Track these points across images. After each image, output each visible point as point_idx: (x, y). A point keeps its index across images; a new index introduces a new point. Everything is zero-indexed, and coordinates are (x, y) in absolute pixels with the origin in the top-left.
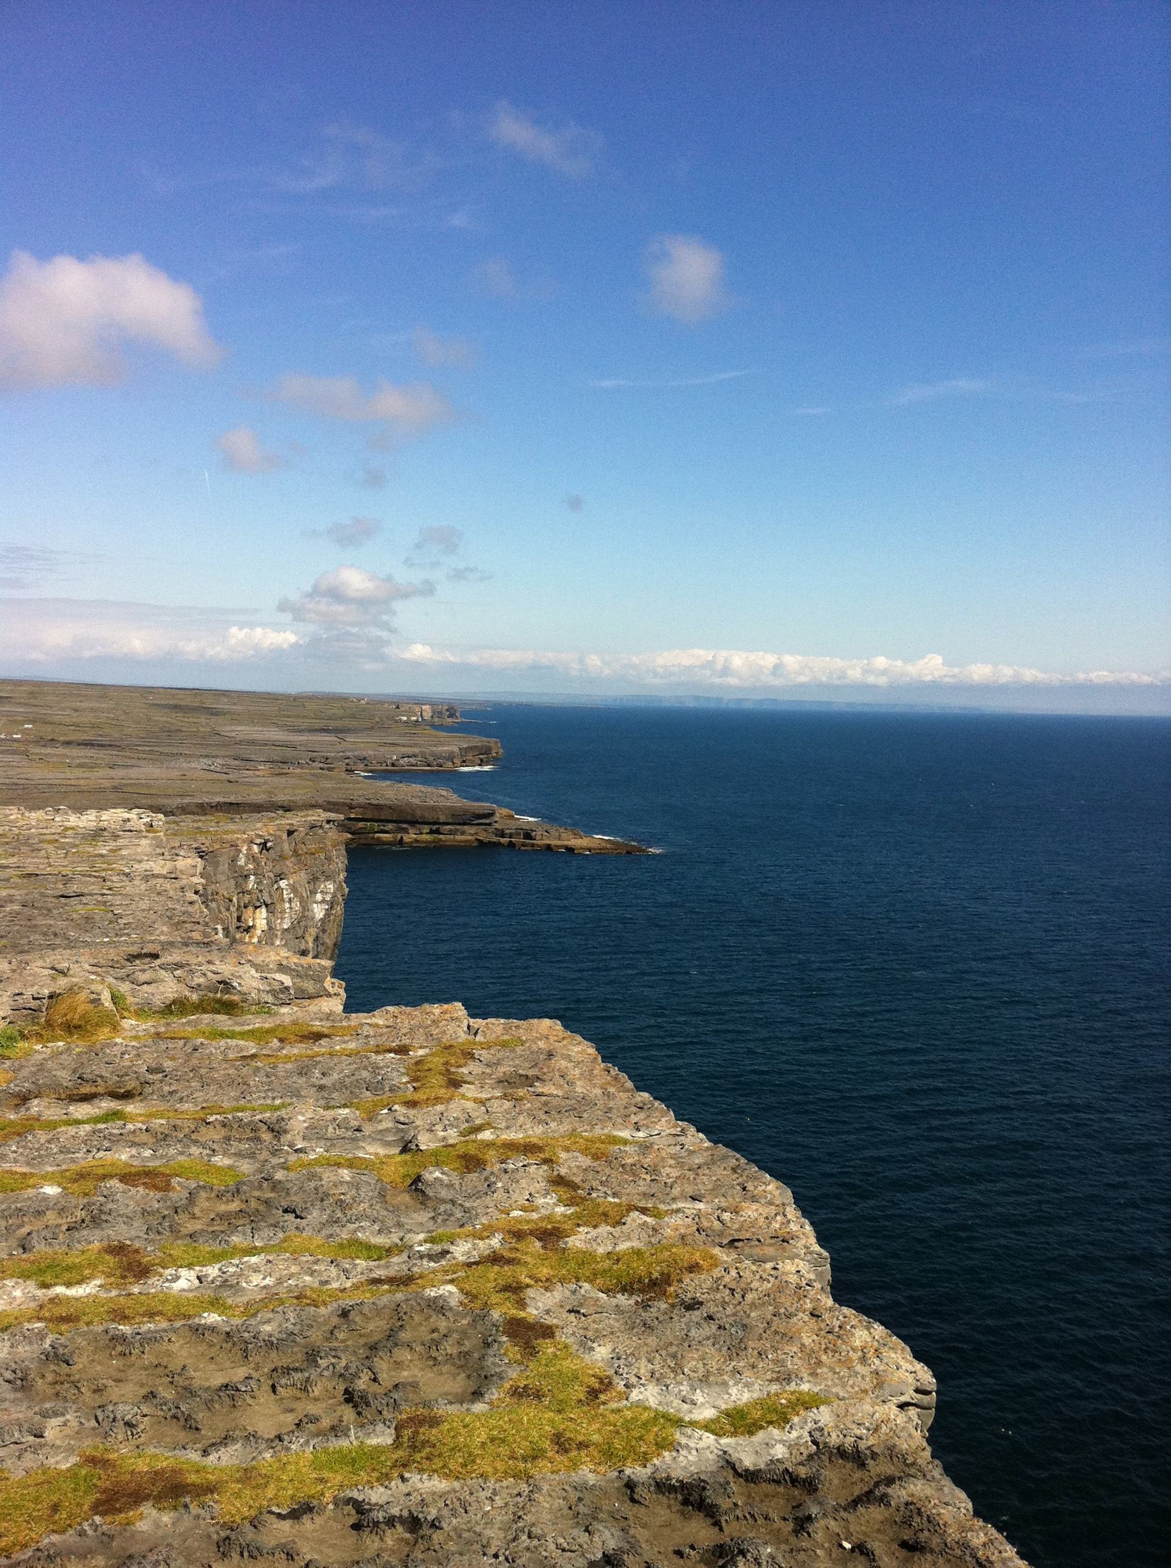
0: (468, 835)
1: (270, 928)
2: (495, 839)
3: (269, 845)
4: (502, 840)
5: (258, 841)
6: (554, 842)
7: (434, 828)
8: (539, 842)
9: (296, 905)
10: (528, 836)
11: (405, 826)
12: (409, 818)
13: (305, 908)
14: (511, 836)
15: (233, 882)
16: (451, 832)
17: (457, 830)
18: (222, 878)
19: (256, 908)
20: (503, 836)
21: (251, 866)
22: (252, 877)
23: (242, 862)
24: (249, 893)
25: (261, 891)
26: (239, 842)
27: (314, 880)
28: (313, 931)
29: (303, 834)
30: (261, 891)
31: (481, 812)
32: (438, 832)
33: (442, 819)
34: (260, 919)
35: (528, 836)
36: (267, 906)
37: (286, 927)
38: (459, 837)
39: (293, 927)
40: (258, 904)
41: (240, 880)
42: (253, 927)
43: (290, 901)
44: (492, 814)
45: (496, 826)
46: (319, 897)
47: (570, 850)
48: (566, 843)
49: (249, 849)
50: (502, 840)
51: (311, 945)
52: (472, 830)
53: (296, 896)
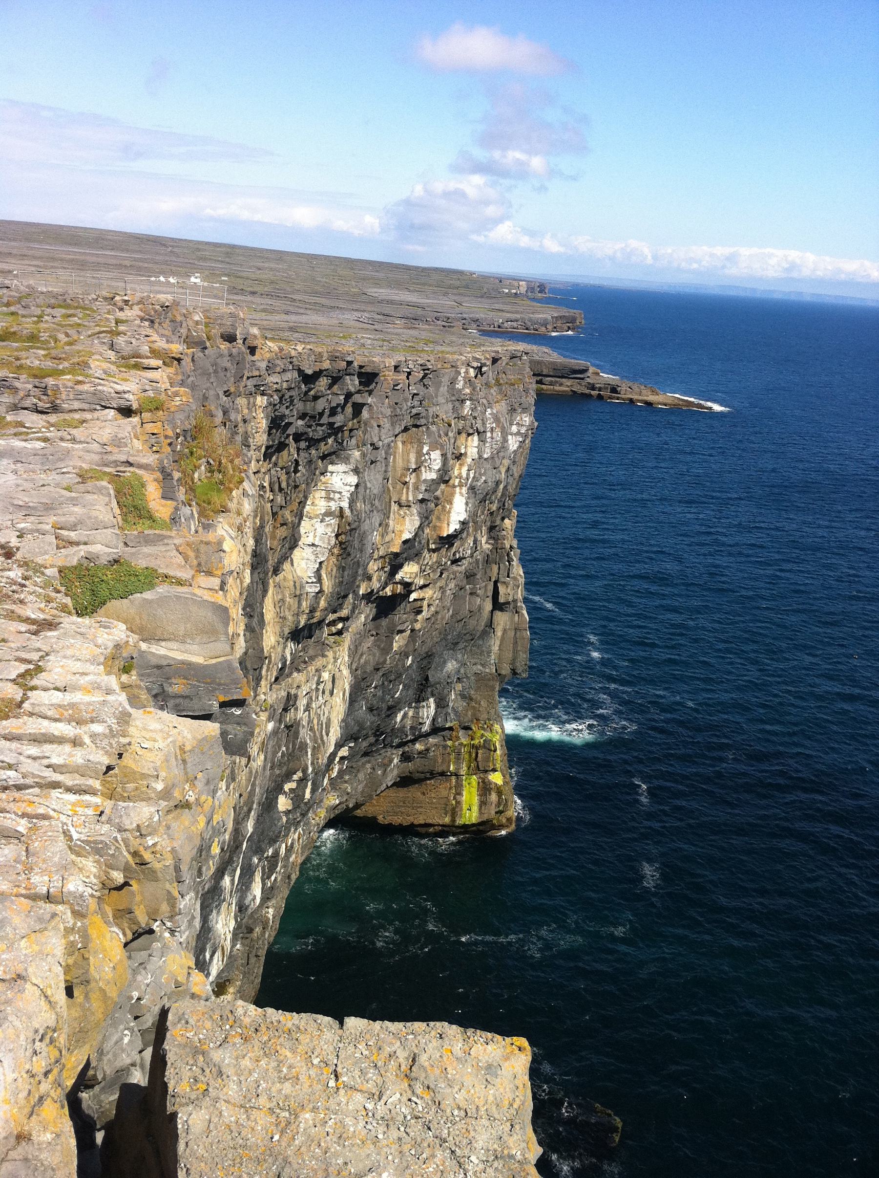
0: (566, 386)
2: (587, 391)
4: (593, 393)
5: (475, 364)
6: (635, 397)
8: (623, 396)
9: (498, 435)
10: (614, 390)
13: (505, 440)
14: (600, 389)
15: (450, 406)
17: (557, 382)
18: (441, 400)
19: (469, 435)
20: (593, 388)
21: (468, 391)
22: (468, 403)
23: (460, 385)
24: (464, 418)
25: (475, 418)
27: (512, 410)
28: (506, 462)
31: (577, 368)
33: (545, 372)
34: (471, 447)
35: (614, 390)
36: (479, 433)
38: (557, 388)
40: (471, 431)
41: (457, 404)
42: (466, 453)
44: (585, 371)
45: (588, 380)
46: (514, 429)
47: (649, 404)
48: (645, 398)
49: (467, 372)
50: (593, 393)
52: (568, 382)
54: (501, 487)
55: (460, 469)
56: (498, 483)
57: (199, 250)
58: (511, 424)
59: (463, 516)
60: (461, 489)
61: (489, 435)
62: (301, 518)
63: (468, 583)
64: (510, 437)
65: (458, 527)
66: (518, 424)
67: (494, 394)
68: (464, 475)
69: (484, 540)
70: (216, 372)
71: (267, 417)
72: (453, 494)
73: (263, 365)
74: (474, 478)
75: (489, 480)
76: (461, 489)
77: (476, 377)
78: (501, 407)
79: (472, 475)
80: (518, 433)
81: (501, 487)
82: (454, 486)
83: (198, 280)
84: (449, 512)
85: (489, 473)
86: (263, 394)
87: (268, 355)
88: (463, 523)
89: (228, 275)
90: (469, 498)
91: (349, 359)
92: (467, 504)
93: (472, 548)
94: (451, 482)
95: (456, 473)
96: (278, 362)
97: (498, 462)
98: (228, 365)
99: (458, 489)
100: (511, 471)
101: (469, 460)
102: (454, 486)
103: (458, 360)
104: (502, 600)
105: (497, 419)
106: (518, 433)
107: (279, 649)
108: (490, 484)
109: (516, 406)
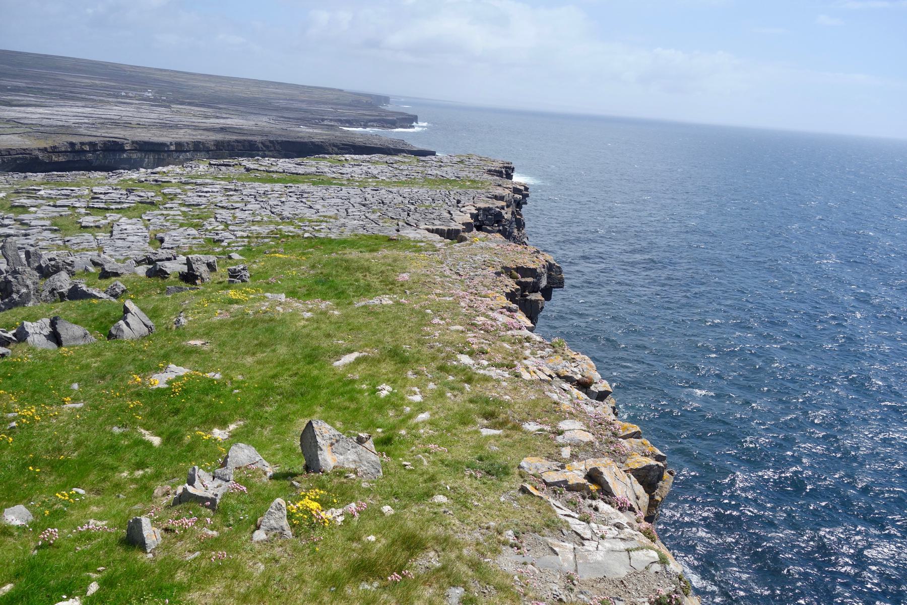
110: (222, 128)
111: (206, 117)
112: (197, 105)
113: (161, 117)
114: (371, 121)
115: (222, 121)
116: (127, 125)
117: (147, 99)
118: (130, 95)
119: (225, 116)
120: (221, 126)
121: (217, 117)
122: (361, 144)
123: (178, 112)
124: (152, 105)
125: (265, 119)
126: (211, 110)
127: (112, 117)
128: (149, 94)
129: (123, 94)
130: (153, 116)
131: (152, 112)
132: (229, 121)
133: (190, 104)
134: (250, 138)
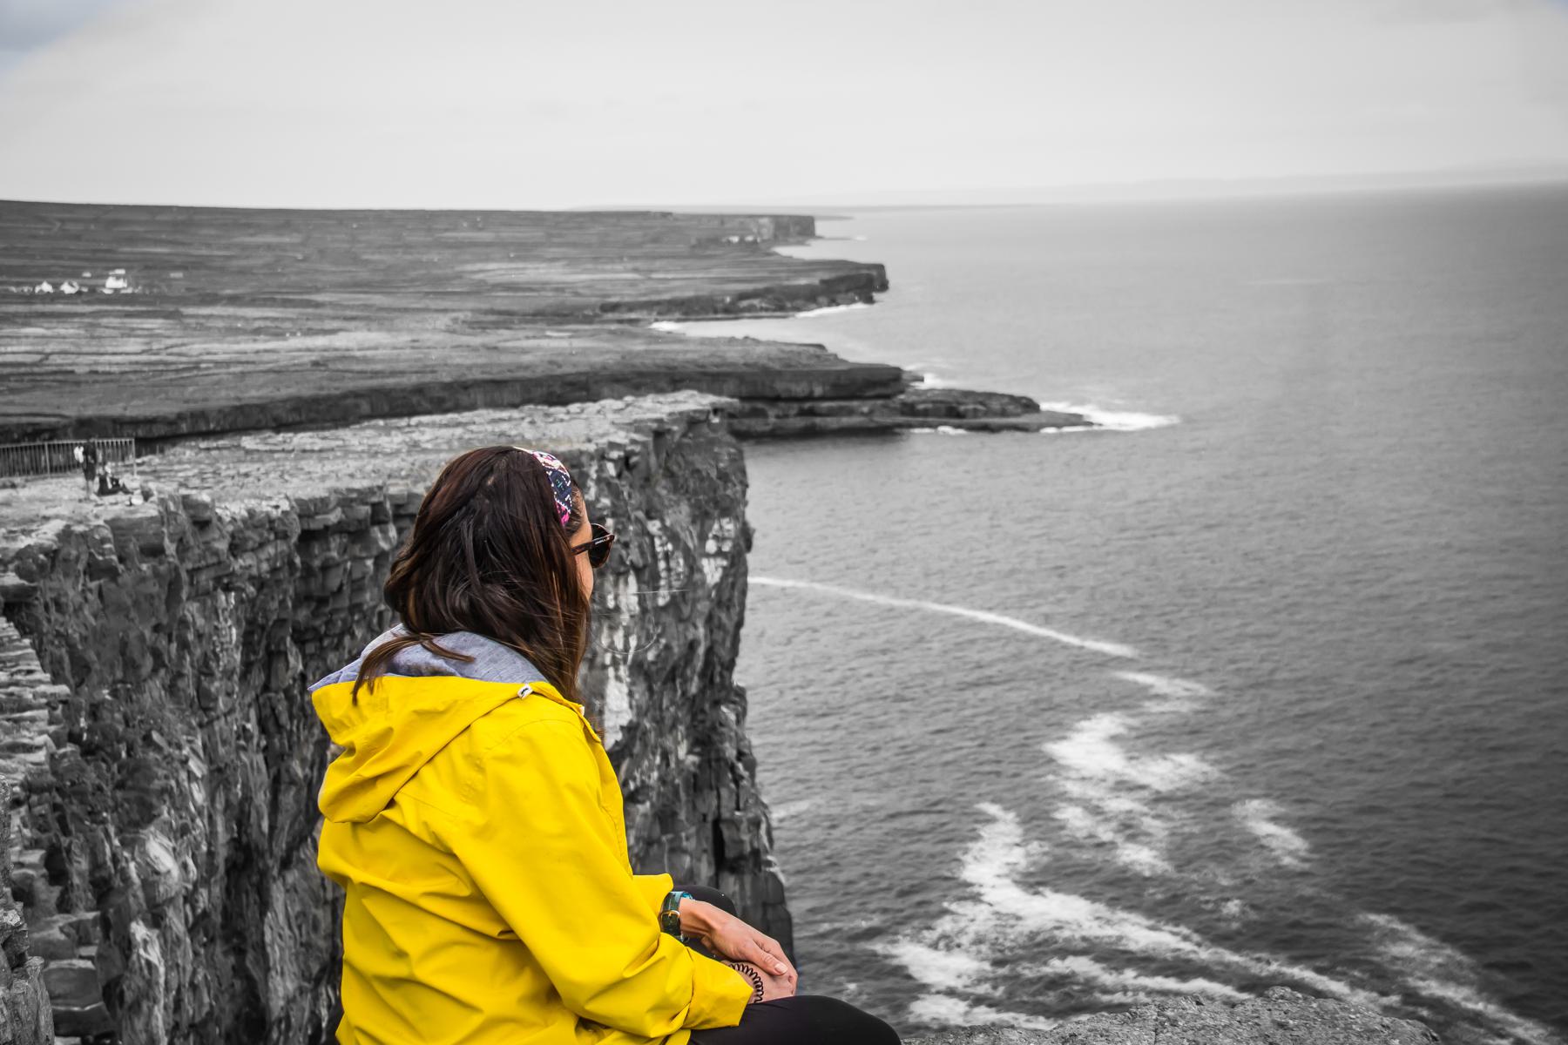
1: (644, 611)
3: (634, 459)
5: (615, 454)
7: (807, 405)
9: (680, 565)
11: (760, 405)
12: (768, 393)
13: (693, 568)
16: (830, 413)
19: (618, 574)
26: (584, 459)
28: (703, 607)
29: (677, 437)
30: (626, 545)
32: (812, 413)
37: (661, 602)
39: (674, 603)
40: (622, 569)
42: (617, 609)
43: (667, 557)
49: (601, 469)
51: (701, 631)
53: (676, 547)
54: (701, 650)
55: (611, 636)
56: (692, 646)
57: (116, 222)
58: (703, 538)
59: (626, 718)
60: (617, 670)
61: (662, 565)
62: (323, 767)
63: (664, 831)
64: (705, 562)
65: (619, 737)
66: (716, 537)
67: (664, 492)
68: (619, 645)
69: (682, 751)
70: (136, 603)
71: (238, 623)
72: (603, 681)
73: (222, 546)
74: (638, 647)
75: (674, 644)
76: (617, 670)
77: (619, 476)
78: (679, 515)
79: (633, 642)
80: (719, 553)
81: (701, 650)
82: (605, 667)
83: (121, 284)
84: (601, 712)
85: (672, 630)
86: (227, 589)
87: (230, 528)
88: (630, 730)
89: (182, 267)
90: (633, 684)
91: (375, 499)
92: (631, 694)
93: (659, 767)
94: (599, 660)
95: (605, 642)
96: (249, 533)
97: (686, 611)
98: (155, 589)
99: (611, 672)
100: (716, 621)
101: (625, 618)
102: (605, 667)
103: (581, 453)
104: (730, 853)
105: (673, 537)
106: (719, 553)
107: (306, 1003)
108: (676, 650)
109: (710, 508)
110: (316, 364)
111: (279, 334)
112: (253, 302)
113: (155, 346)
114: (743, 296)
115: (320, 341)
116: (65, 379)
117: (117, 298)
118: (67, 288)
119: (329, 325)
120: (314, 357)
121: (310, 332)
122: (691, 368)
123: (202, 329)
124: (129, 315)
125: (443, 321)
126: (291, 312)
127: (20, 358)
128: (112, 284)
129: (46, 287)
130: (133, 345)
131: (131, 333)
132: (341, 341)
133: (234, 300)
134: (391, 382)
